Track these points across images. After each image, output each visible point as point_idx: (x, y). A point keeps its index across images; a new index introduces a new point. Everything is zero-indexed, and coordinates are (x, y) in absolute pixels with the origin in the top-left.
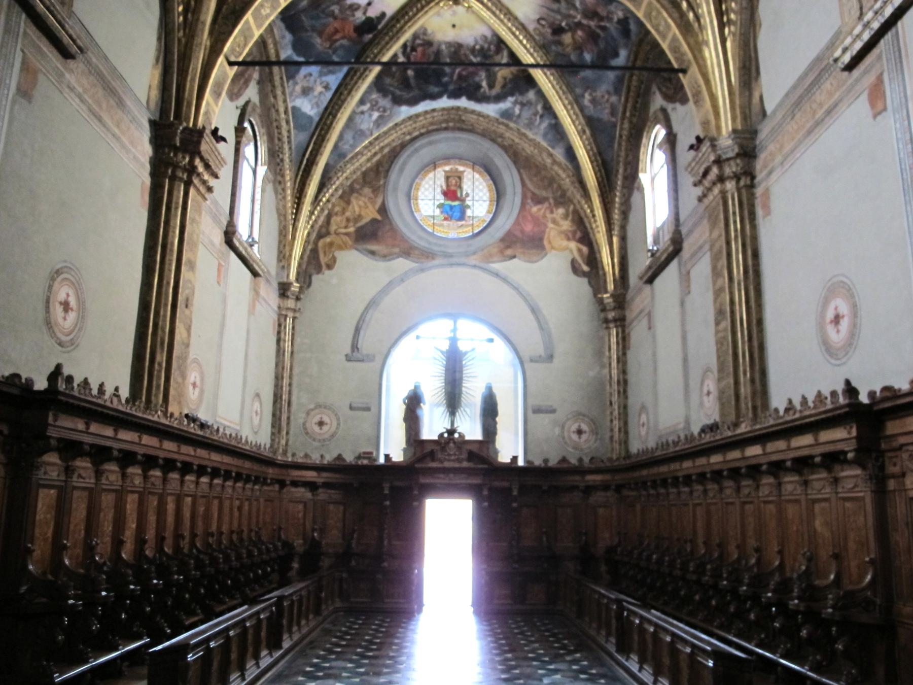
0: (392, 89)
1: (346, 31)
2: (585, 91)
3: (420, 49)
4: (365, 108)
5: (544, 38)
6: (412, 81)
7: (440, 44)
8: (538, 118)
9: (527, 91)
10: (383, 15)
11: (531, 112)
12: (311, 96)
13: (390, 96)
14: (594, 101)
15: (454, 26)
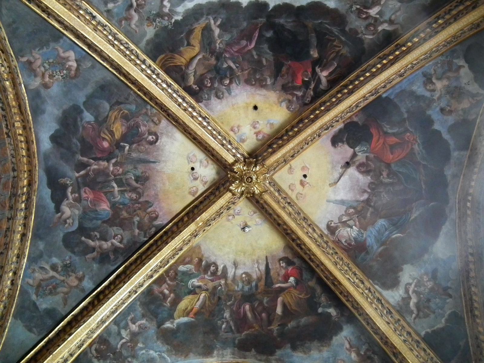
0: (343, 38)
1: (381, 141)
2: (77, 69)
3: (299, 83)
4: (385, 27)
5: (146, 114)
6: (314, 41)
7: (273, 87)
8: (135, 4)
9: (156, 35)
10: (335, 141)
11: (147, 8)
12: (455, 84)
13: (347, 29)
14: (61, 62)
15: (255, 108)
